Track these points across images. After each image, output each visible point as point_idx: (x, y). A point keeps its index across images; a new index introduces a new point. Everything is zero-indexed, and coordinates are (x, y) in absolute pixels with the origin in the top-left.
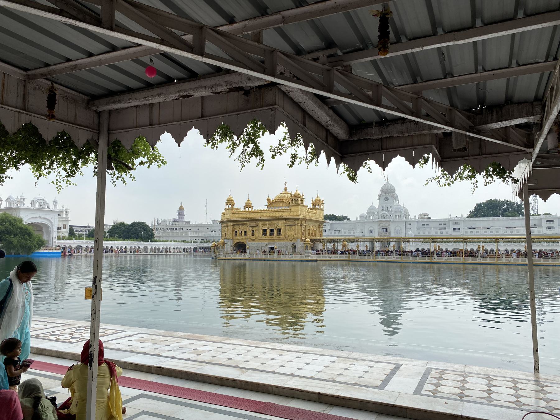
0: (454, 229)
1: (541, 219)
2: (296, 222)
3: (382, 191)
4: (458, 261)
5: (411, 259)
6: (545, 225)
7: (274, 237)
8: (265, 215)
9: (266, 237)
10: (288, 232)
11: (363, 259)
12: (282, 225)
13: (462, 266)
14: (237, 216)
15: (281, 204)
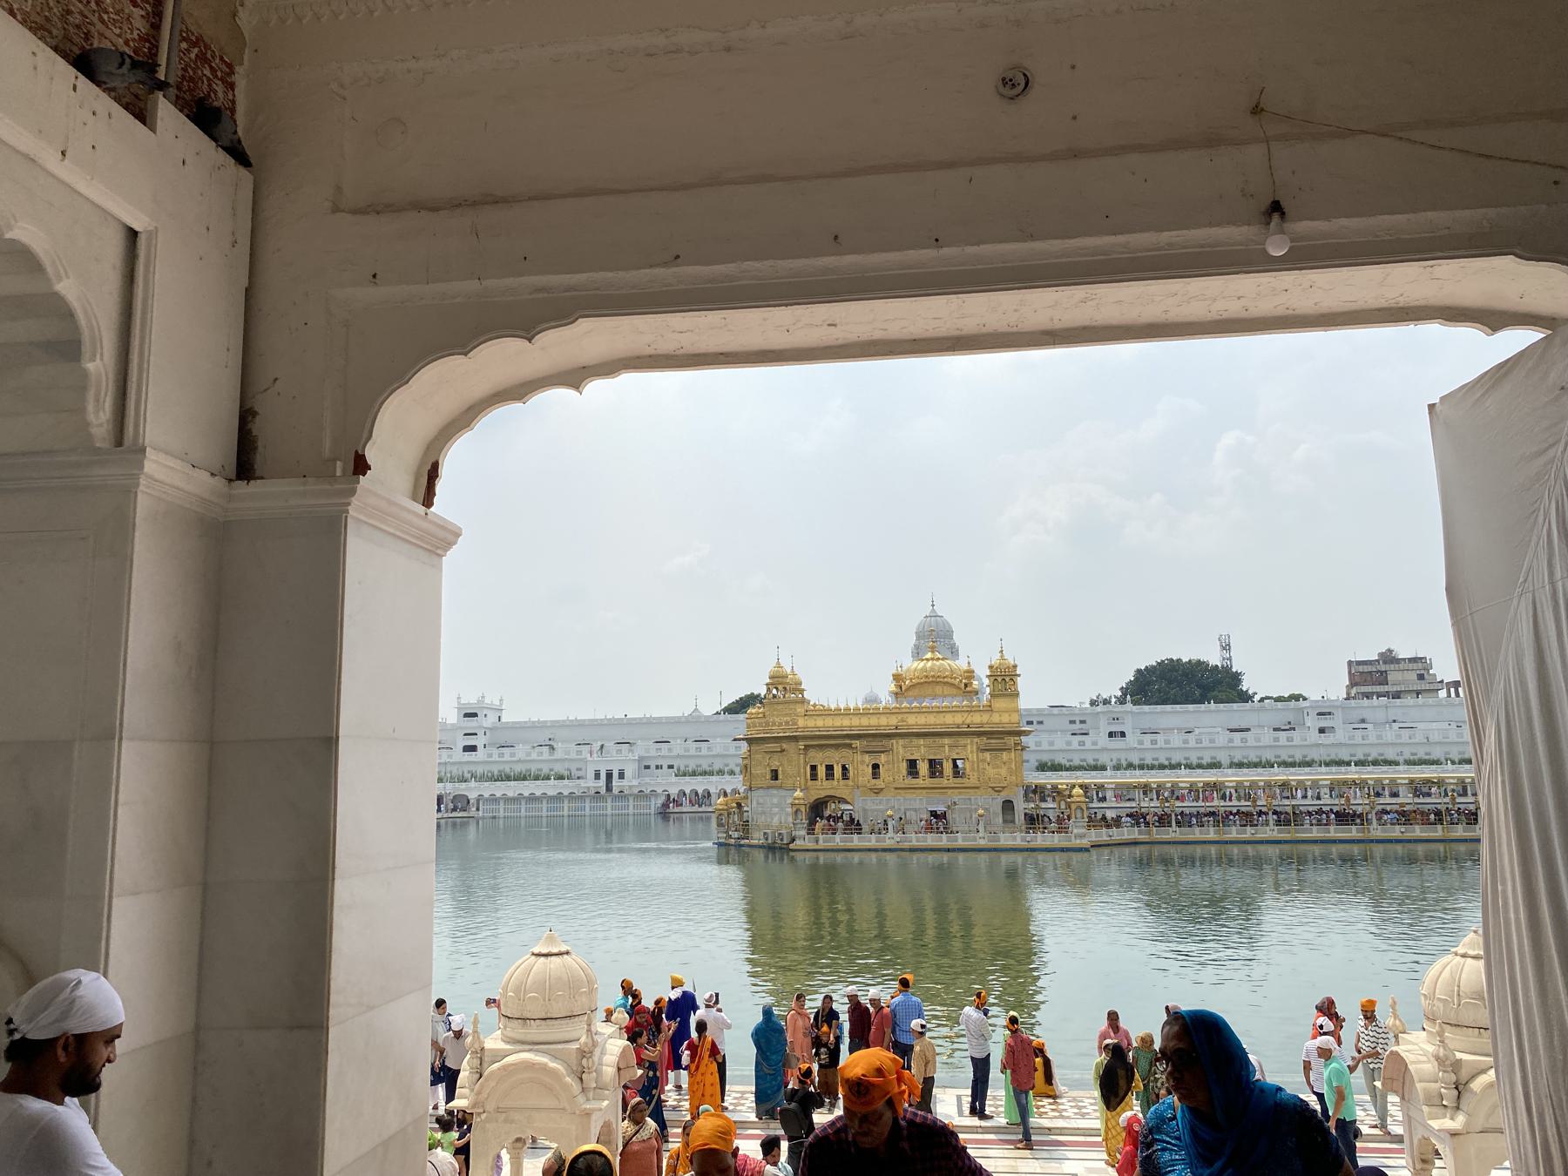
0: (1111, 735)
1: (1302, 710)
2: (1011, 740)
3: (919, 636)
4: (1432, 835)
5: (1316, 833)
6: (1313, 722)
7: (944, 782)
8: (911, 720)
9: (919, 782)
10: (996, 769)
11: (1190, 837)
12: (969, 752)
13: (1441, 847)
14: (820, 722)
15: (938, 690)
